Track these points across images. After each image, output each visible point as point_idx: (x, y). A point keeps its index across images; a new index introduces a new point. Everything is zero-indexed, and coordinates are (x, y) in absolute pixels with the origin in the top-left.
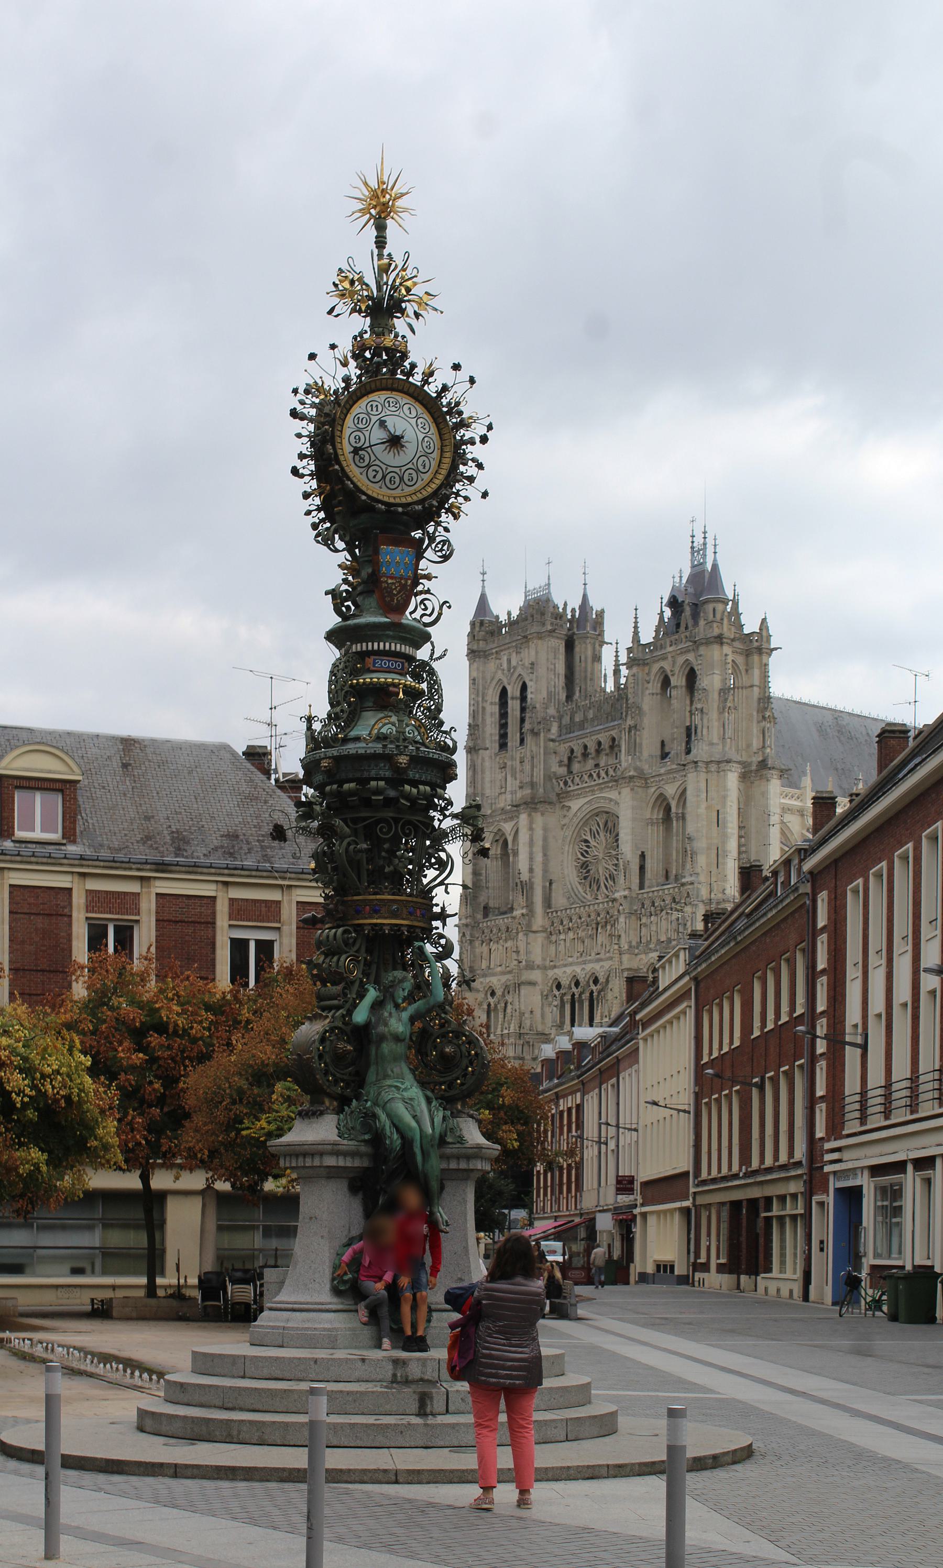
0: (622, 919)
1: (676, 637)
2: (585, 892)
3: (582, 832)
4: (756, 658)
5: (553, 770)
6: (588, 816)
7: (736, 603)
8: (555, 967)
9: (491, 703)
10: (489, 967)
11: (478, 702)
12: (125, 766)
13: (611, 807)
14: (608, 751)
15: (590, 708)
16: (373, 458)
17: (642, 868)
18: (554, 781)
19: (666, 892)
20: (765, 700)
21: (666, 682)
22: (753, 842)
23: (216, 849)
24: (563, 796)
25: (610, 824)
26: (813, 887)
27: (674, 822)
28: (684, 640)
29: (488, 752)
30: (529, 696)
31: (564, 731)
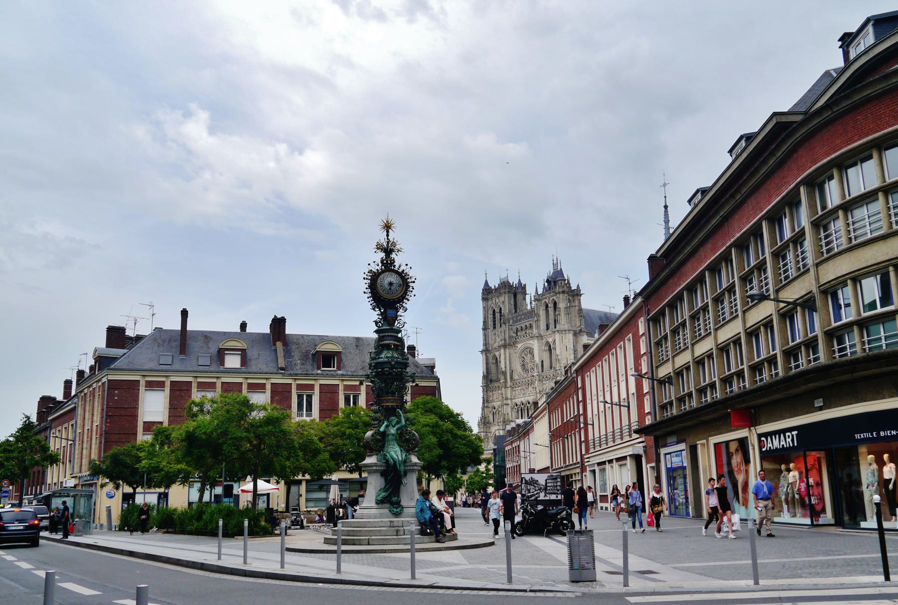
0: (536, 382)
4: (576, 297)
8: (515, 399)
10: (493, 400)
13: (531, 346)
17: (542, 365)
20: (580, 310)
21: (547, 306)
24: (515, 343)
25: (531, 352)
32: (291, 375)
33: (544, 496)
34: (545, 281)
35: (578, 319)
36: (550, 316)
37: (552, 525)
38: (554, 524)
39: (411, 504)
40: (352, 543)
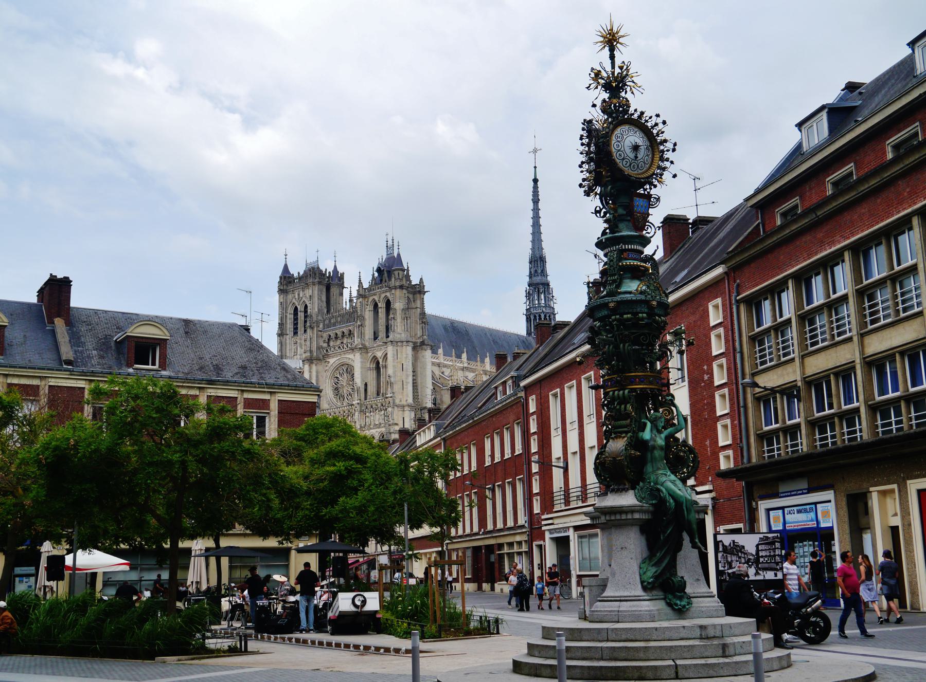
0: (357, 414)
4: (418, 295)
5: (321, 344)
7: (408, 270)
12: (186, 333)
13: (351, 362)
16: (626, 155)
17: (366, 390)
20: (423, 314)
21: (376, 306)
22: (419, 378)
23: (237, 374)
24: (326, 356)
25: (350, 370)
26: (526, 394)
30: (309, 311)
31: (326, 327)
32: (83, 373)
33: (755, 575)
34: (375, 269)
35: (419, 327)
36: (380, 321)
37: (796, 624)
38: (799, 623)
39: (700, 591)
40: (636, 675)
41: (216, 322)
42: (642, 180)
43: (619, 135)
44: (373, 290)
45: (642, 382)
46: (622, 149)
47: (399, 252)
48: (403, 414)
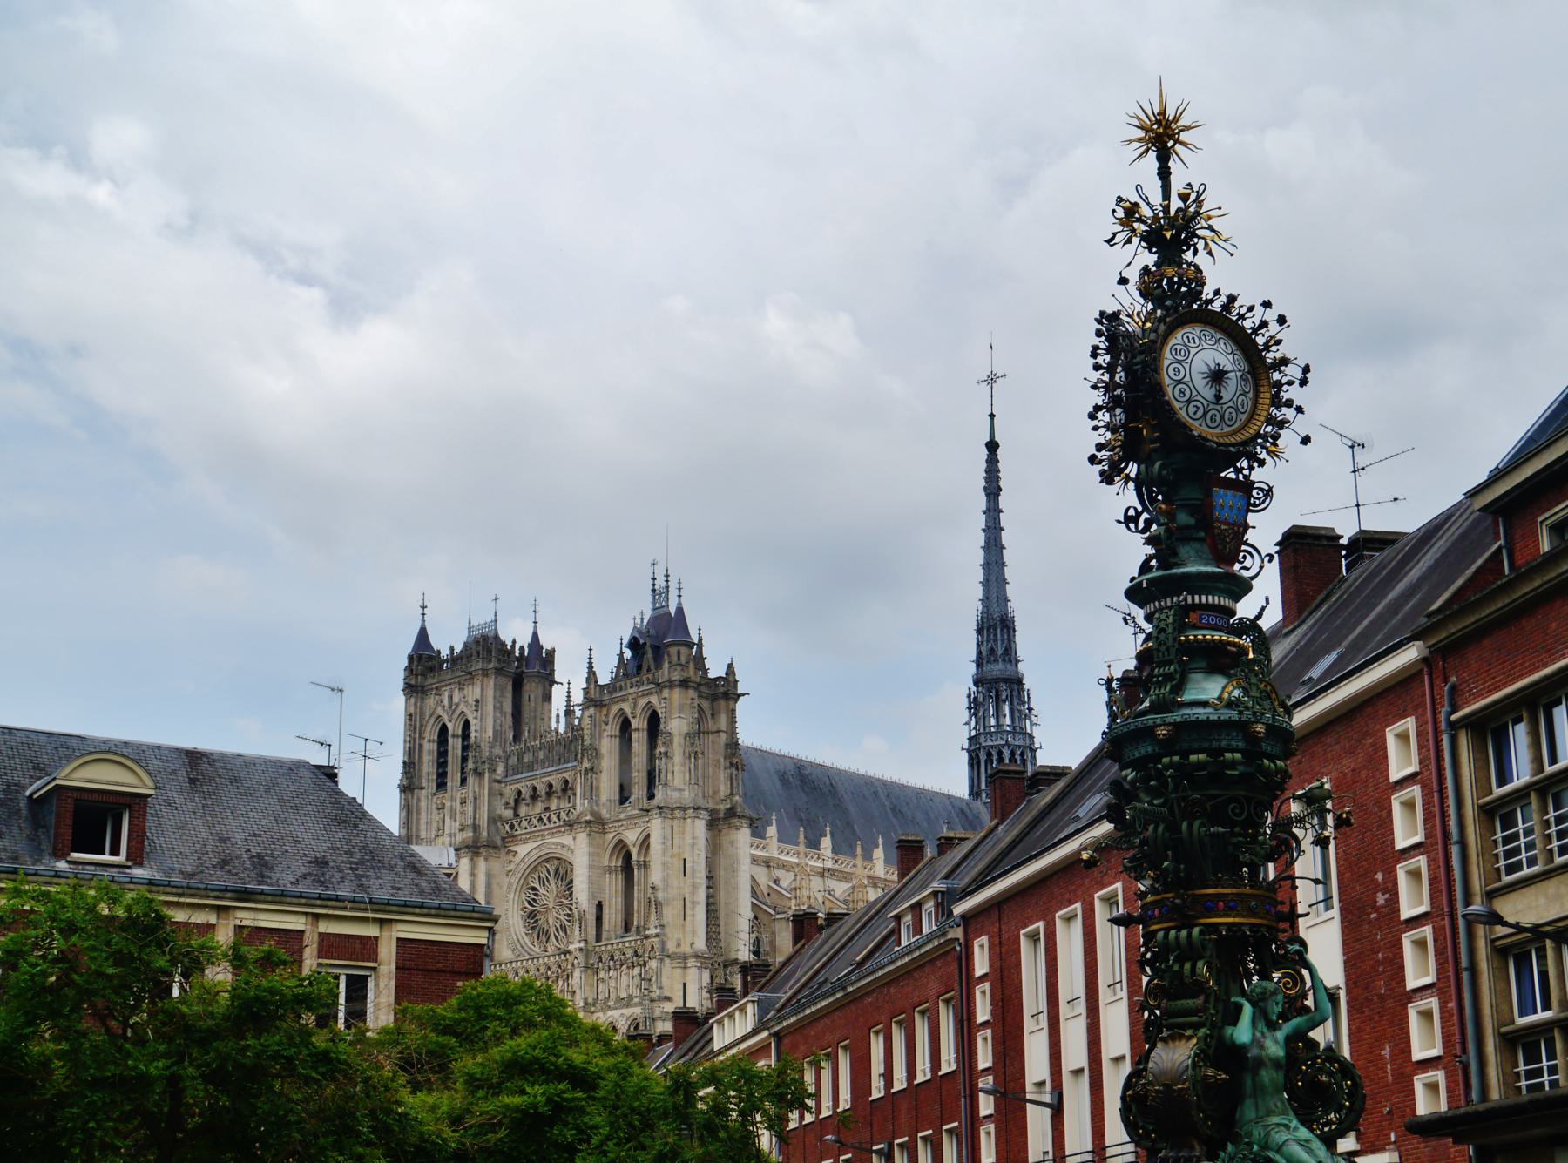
0: (577, 973)
1: (638, 679)
2: (532, 944)
3: (530, 879)
4: (723, 703)
5: (498, 812)
6: (537, 862)
7: (700, 645)
9: (429, 741)
11: (414, 739)
12: (192, 781)
13: (565, 854)
14: (559, 794)
15: (540, 749)
16: (1194, 393)
17: (599, 919)
18: (499, 824)
19: (627, 945)
20: (733, 745)
21: (625, 726)
23: (304, 876)
24: (510, 839)
25: (562, 872)
26: (966, 933)
27: (636, 871)
28: (646, 682)
29: (424, 791)
30: (473, 735)
31: (511, 772)
34: (625, 642)
35: (723, 775)
41: (260, 758)
42: (1233, 449)
43: (1179, 347)
44: (621, 689)
45: (1232, 909)
46: (1187, 378)
47: (680, 603)
48: (684, 976)
